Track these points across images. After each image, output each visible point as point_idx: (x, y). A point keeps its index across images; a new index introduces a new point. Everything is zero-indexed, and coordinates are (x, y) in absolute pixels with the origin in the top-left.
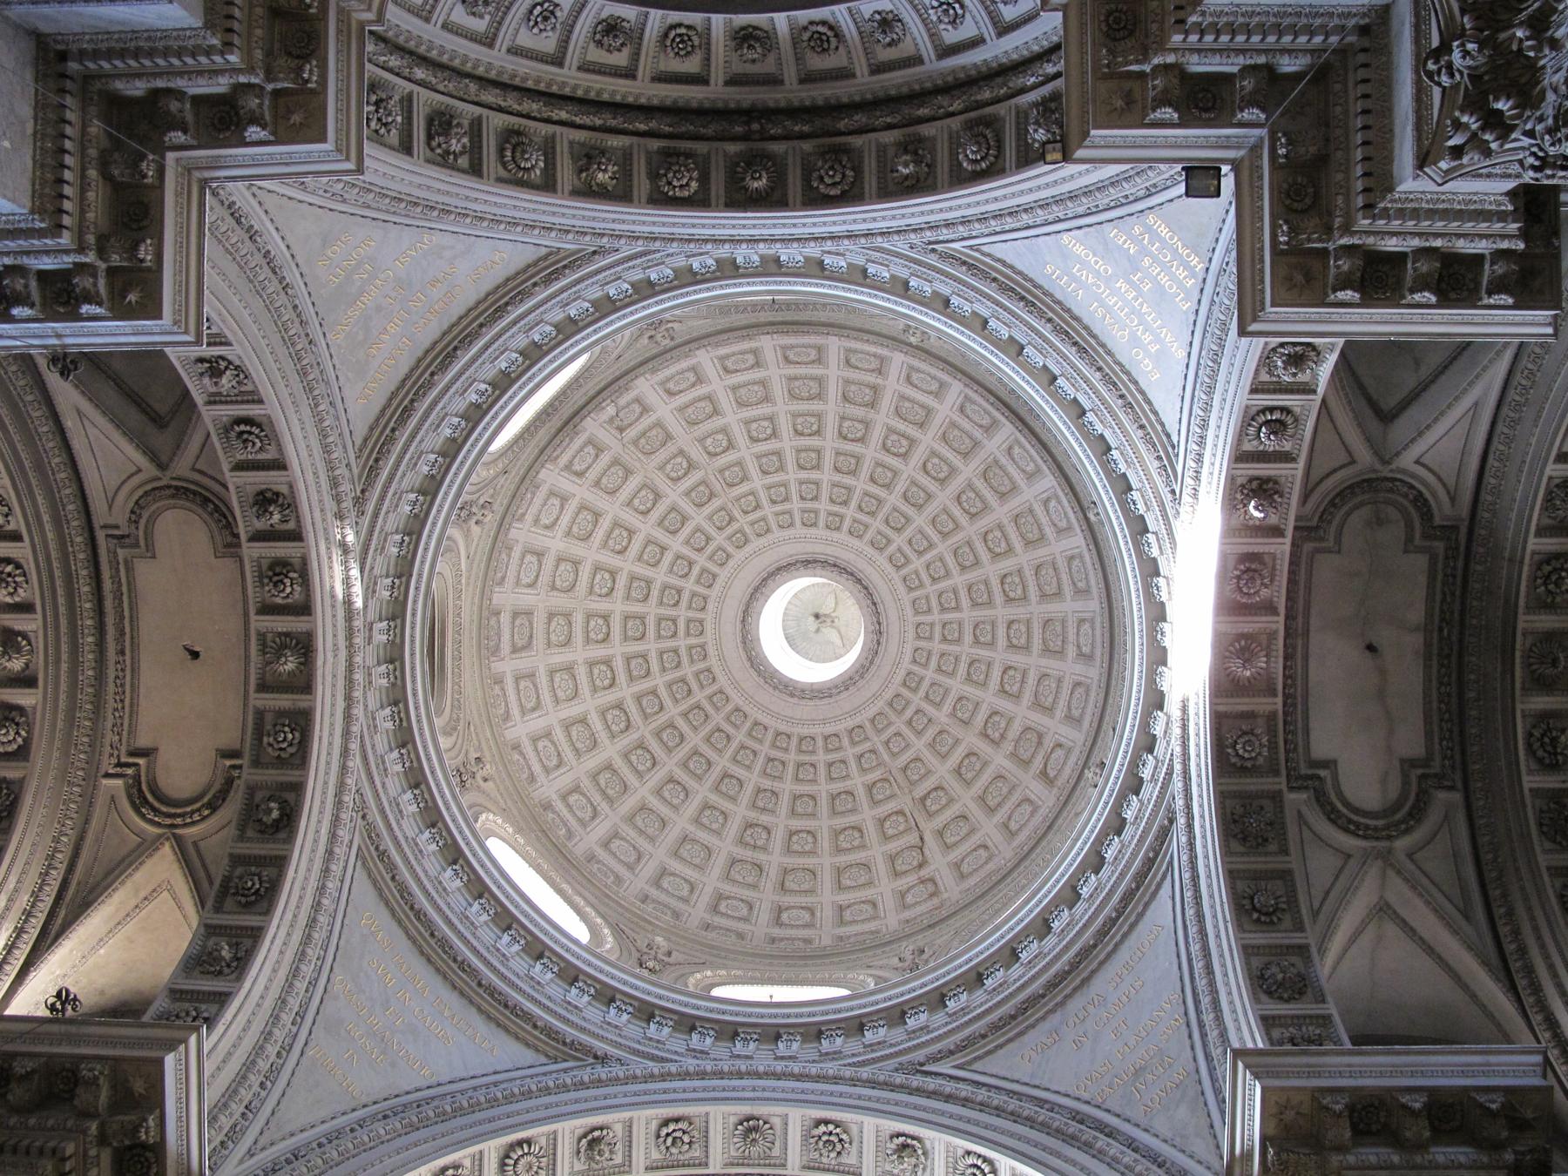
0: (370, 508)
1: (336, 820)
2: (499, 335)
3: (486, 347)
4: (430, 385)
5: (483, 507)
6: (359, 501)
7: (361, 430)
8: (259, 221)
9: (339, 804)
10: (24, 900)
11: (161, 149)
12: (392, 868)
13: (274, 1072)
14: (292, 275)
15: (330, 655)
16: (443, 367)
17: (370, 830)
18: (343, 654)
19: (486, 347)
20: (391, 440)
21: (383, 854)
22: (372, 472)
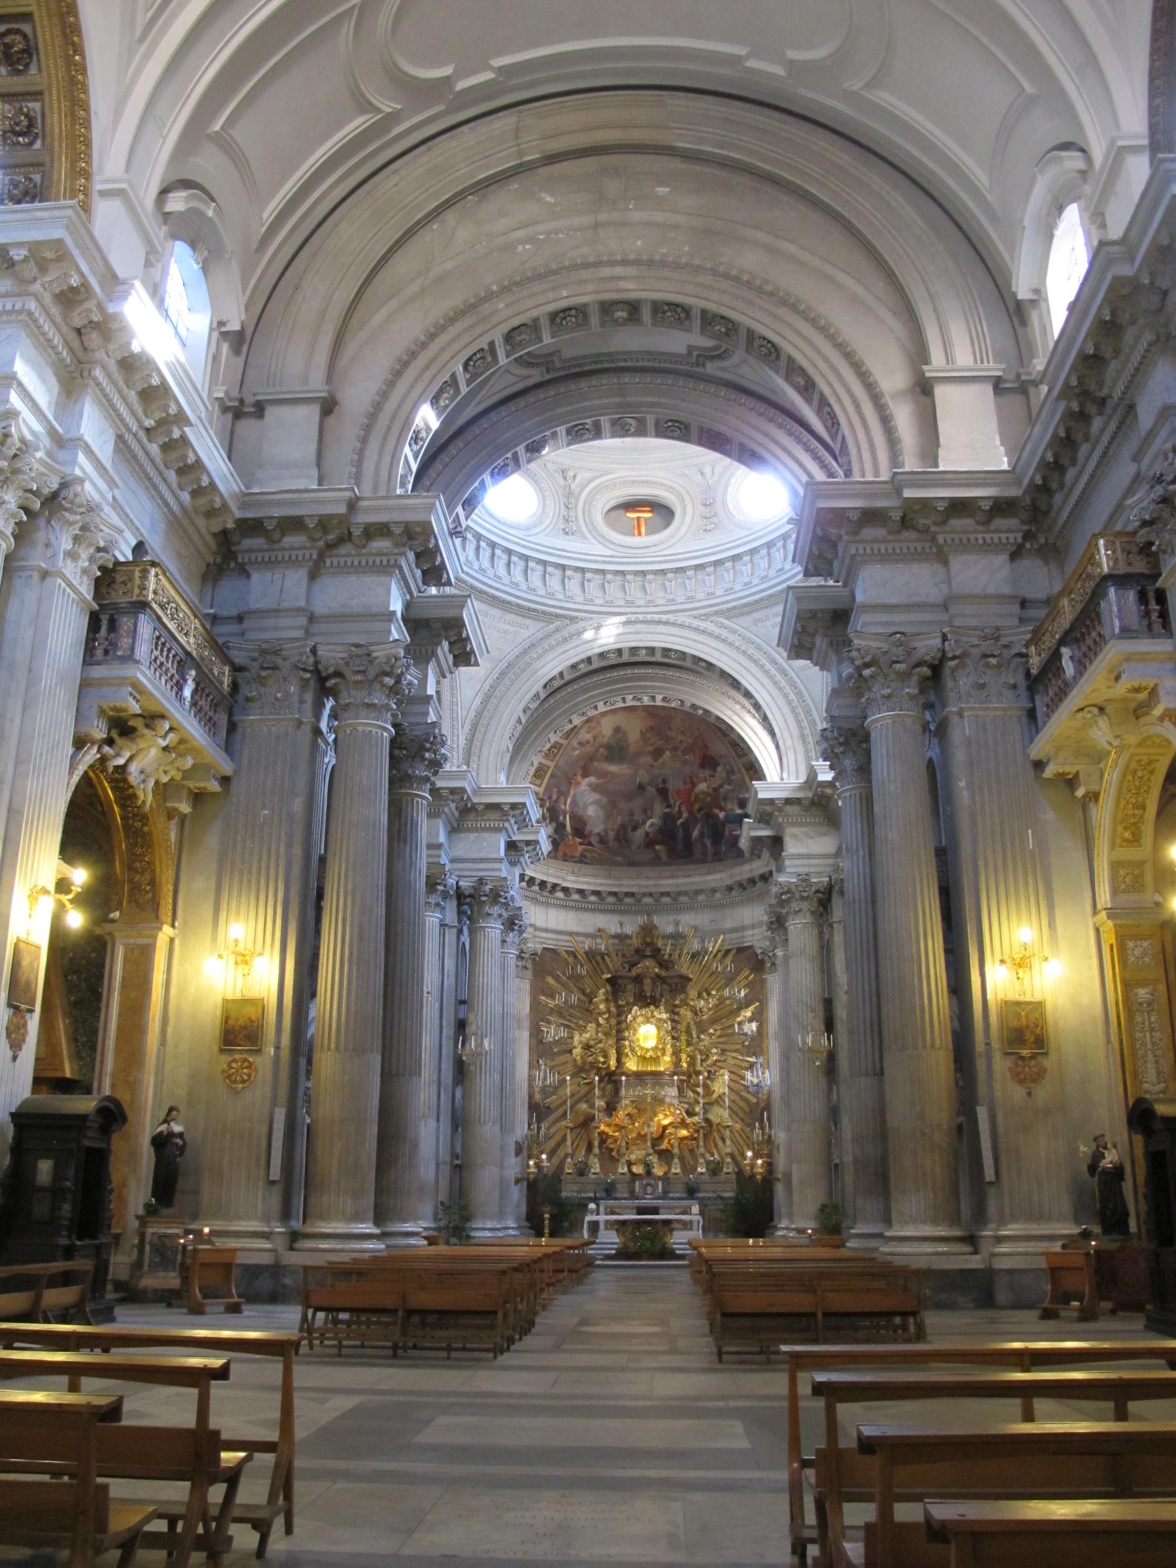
0: (574, 614)
1: (710, 635)
2: (491, 587)
3: (497, 589)
4: (518, 605)
5: (565, 479)
6: (573, 619)
7: (541, 624)
8: (472, 714)
9: (704, 632)
10: (738, 707)
11: (474, 805)
12: (735, 608)
13: (799, 694)
14: (487, 687)
15: (640, 636)
16: (509, 603)
17: (716, 613)
18: (640, 626)
19: (497, 589)
20: (543, 612)
21: (729, 610)
22: (557, 616)
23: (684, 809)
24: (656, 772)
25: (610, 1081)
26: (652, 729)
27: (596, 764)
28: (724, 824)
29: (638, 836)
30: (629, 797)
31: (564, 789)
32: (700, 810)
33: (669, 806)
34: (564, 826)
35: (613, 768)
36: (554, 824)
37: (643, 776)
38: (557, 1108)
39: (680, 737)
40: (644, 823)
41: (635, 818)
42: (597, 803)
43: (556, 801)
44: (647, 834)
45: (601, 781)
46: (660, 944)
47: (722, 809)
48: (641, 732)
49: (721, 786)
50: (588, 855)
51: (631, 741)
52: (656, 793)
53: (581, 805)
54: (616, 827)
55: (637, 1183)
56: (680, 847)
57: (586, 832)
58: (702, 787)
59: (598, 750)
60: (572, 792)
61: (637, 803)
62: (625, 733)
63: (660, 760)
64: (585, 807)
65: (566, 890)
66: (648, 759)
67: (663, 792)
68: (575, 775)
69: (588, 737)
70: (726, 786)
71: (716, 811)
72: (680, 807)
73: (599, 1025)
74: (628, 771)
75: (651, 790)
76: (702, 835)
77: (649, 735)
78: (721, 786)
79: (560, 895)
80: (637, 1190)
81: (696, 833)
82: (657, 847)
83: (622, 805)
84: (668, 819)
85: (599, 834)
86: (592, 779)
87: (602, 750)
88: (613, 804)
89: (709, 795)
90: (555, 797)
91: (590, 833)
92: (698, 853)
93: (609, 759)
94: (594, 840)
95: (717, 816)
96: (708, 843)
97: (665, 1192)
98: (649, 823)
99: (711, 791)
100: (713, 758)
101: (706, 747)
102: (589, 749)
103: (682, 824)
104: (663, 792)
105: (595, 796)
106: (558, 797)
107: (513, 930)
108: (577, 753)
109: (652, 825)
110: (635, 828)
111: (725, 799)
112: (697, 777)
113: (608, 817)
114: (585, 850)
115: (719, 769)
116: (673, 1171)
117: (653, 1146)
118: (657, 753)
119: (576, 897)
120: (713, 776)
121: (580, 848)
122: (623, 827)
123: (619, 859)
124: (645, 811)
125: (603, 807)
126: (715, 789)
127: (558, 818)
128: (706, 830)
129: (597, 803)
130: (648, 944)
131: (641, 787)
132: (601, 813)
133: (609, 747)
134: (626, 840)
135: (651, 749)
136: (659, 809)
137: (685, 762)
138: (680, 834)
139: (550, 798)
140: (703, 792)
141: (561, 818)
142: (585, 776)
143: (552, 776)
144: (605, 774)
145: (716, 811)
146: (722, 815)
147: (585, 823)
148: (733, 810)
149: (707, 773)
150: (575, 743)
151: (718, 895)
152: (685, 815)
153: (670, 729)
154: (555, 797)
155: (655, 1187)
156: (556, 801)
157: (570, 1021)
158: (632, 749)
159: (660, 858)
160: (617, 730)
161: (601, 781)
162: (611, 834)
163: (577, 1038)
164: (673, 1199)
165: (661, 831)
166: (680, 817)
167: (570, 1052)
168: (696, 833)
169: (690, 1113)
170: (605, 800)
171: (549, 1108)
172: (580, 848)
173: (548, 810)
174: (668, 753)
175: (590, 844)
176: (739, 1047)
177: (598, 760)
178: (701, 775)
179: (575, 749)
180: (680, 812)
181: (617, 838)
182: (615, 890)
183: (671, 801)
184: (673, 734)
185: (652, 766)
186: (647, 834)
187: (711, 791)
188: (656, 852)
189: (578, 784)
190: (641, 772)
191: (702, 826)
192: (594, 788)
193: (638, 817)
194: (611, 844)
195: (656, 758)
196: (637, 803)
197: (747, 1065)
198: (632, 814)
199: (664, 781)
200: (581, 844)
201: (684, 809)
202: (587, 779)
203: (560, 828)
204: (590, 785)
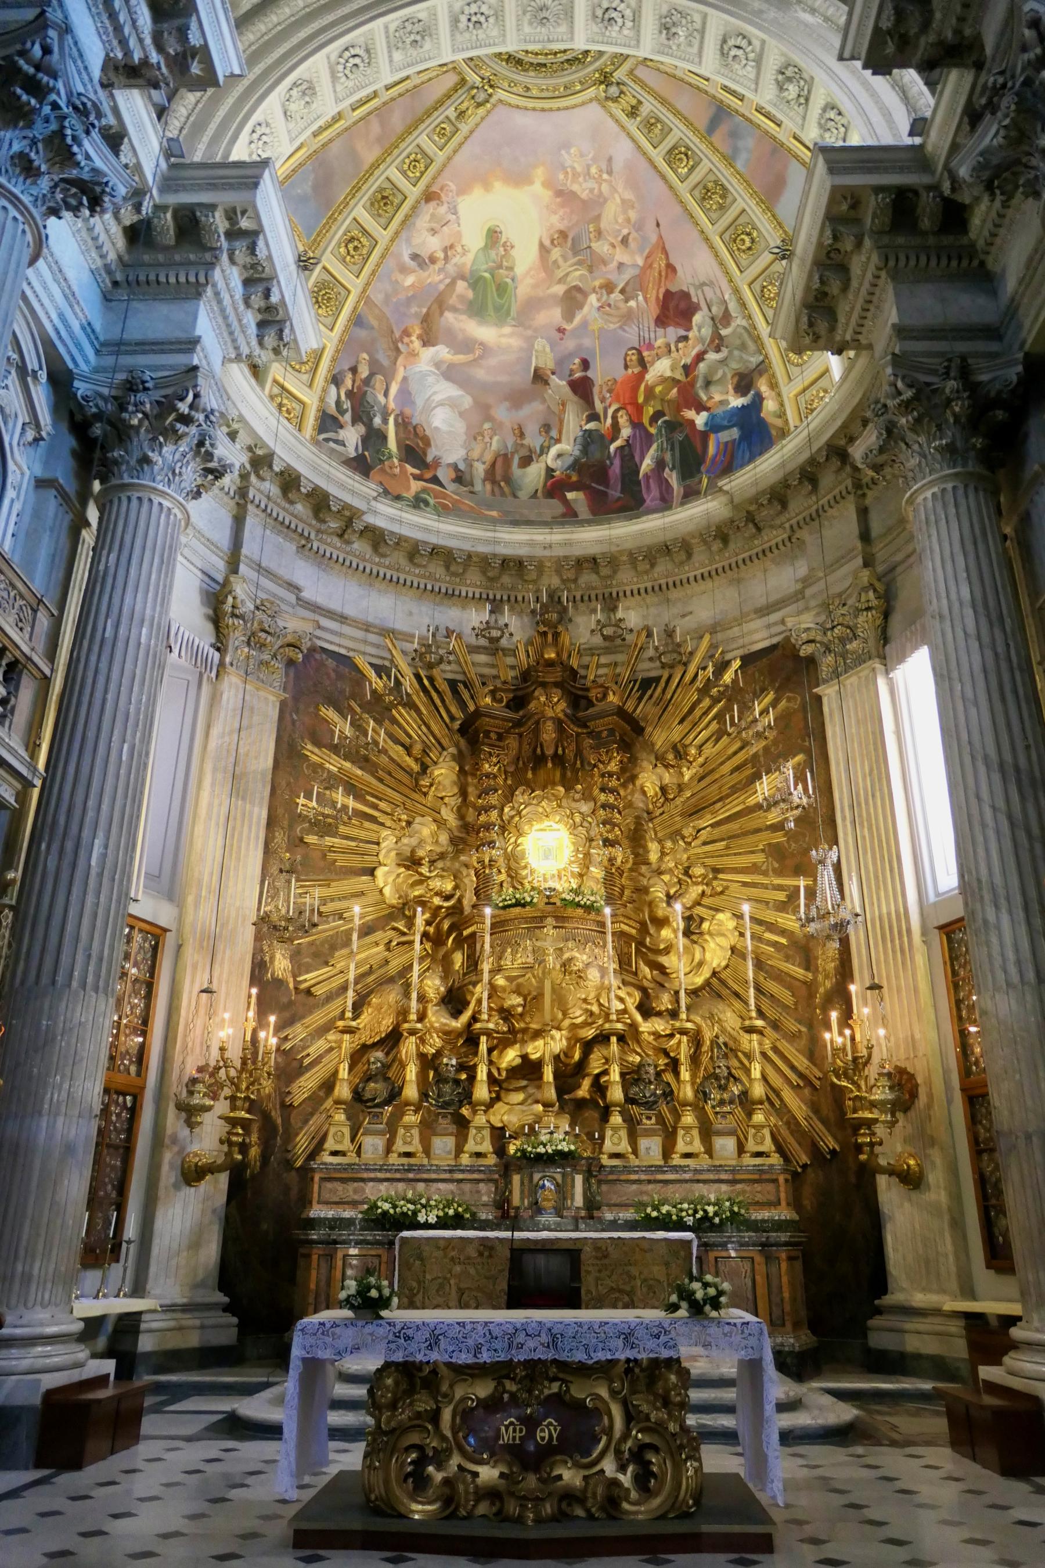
23: (623, 420)
24: (570, 344)
25: (459, 943)
26: (563, 234)
27: (449, 316)
28: (705, 436)
29: (533, 476)
30: (517, 399)
31: (385, 362)
32: (654, 418)
33: (594, 417)
34: (383, 438)
35: (485, 333)
36: (361, 429)
37: (544, 356)
38: (329, 998)
39: (621, 255)
40: (544, 450)
41: (525, 442)
42: (451, 403)
43: (367, 381)
44: (550, 471)
45: (461, 358)
46: (574, 663)
47: (700, 407)
48: (542, 245)
49: (700, 357)
50: (432, 501)
51: (519, 270)
52: (568, 389)
53: (420, 403)
54: (488, 457)
55: (516, 1179)
56: (615, 493)
57: (429, 459)
58: (661, 368)
59: (453, 283)
60: (401, 373)
61: (531, 413)
62: (508, 247)
63: (578, 319)
64: (429, 408)
65: (376, 537)
66: (555, 315)
67: (582, 388)
68: (406, 333)
69: (433, 244)
70: (712, 356)
71: (690, 414)
72: (614, 418)
73: (440, 823)
74: (515, 342)
75: (559, 384)
76: (660, 465)
77: (556, 253)
78: (700, 357)
79: (360, 546)
80: (516, 1201)
81: (647, 464)
82: (570, 496)
83: (502, 413)
84: (589, 440)
85: (455, 467)
86: (442, 352)
87: (461, 286)
88: (484, 411)
89: (675, 381)
90: (364, 372)
91: (437, 463)
92: (652, 496)
93: (477, 309)
94: (444, 474)
95: (692, 423)
96: (673, 478)
97: (592, 1206)
98: (554, 451)
99: (679, 375)
100: (686, 295)
101: (671, 268)
102: (434, 277)
103: (620, 449)
104: (582, 388)
105: (447, 390)
106: (372, 375)
107: (178, 438)
108: (409, 280)
109: (559, 456)
110: (526, 461)
111: (708, 384)
112: (650, 347)
113: (475, 435)
114: (424, 490)
115: (697, 318)
116: (608, 1146)
117: (560, 1091)
118: (573, 299)
119: (399, 558)
120: (685, 338)
121: (415, 486)
122: (504, 458)
123: (494, 513)
124: (547, 428)
125: (461, 414)
126: (687, 369)
127: (371, 420)
128: (668, 457)
129: (451, 403)
130: (550, 663)
131: (539, 378)
132: (460, 427)
133: (476, 282)
134: (508, 479)
135: (559, 289)
136: (574, 423)
137: (628, 317)
138: (616, 468)
139: (354, 370)
140: (663, 380)
141: (377, 421)
142: (427, 342)
143: (357, 321)
144: (466, 345)
145: (690, 414)
146: (700, 419)
147: (427, 442)
148: (727, 402)
149: (673, 333)
150: (406, 259)
151: (700, 556)
152: (626, 432)
153: (599, 233)
154: (364, 372)
155: (563, 1191)
156: (367, 381)
157: (375, 807)
158: (523, 290)
159: (575, 515)
160: (493, 236)
161: (461, 358)
162: (480, 469)
163: (388, 840)
164: (614, 1225)
165: (576, 465)
166: (614, 439)
167: (371, 872)
168: (647, 464)
169: (646, 1010)
170: (467, 402)
171: (308, 992)
172: (415, 486)
173: (350, 394)
174: (593, 299)
175: (435, 480)
176: (759, 858)
177: (454, 309)
178: (660, 342)
179: (404, 270)
180: (616, 427)
181: (490, 475)
182: (482, 549)
183: (599, 406)
184: (601, 248)
185: (561, 331)
186: (550, 471)
187: (679, 375)
188: (565, 502)
189: (414, 354)
190: (540, 344)
191: (661, 449)
192: (449, 373)
193: (534, 440)
194: (478, 487)
195: (569, 316)
196: (531, 413)
197: (781, 896)
198: (522, 435)
199: (585, 364)
200: (417, 478)
201: (623, 420)
202: (432, 350)
203: (374, 438)
204: (437, 365)
